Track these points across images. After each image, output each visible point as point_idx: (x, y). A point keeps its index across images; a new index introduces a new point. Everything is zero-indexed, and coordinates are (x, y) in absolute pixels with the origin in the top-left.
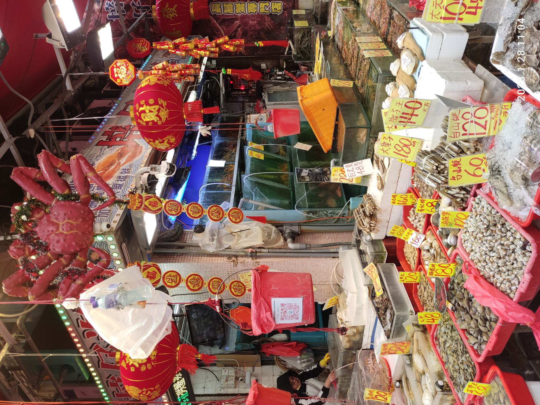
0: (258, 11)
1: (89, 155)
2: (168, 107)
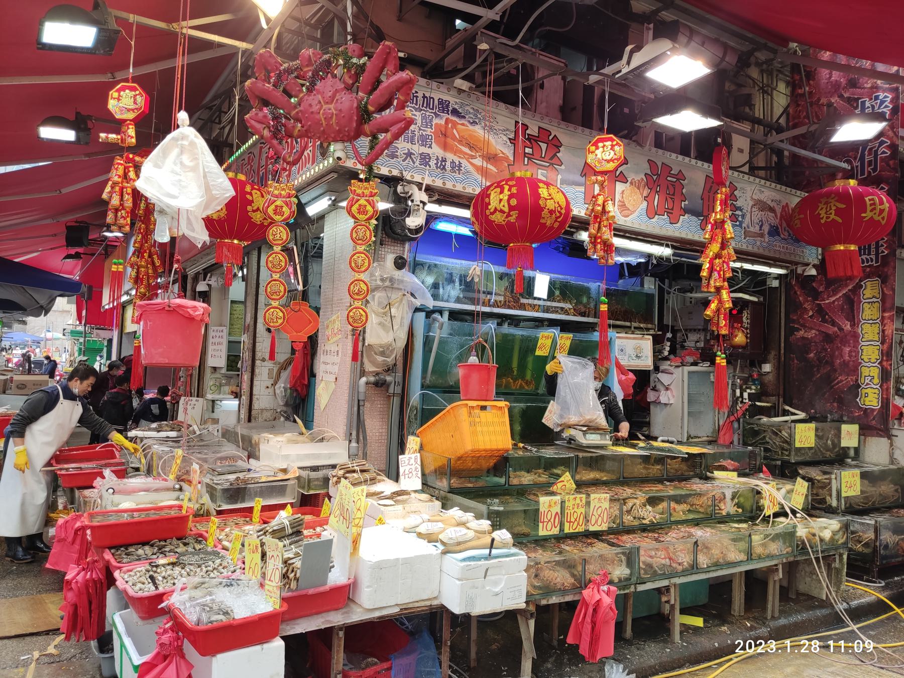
0: (864, 364)
1: (495, 115)
2: (509, 223)
